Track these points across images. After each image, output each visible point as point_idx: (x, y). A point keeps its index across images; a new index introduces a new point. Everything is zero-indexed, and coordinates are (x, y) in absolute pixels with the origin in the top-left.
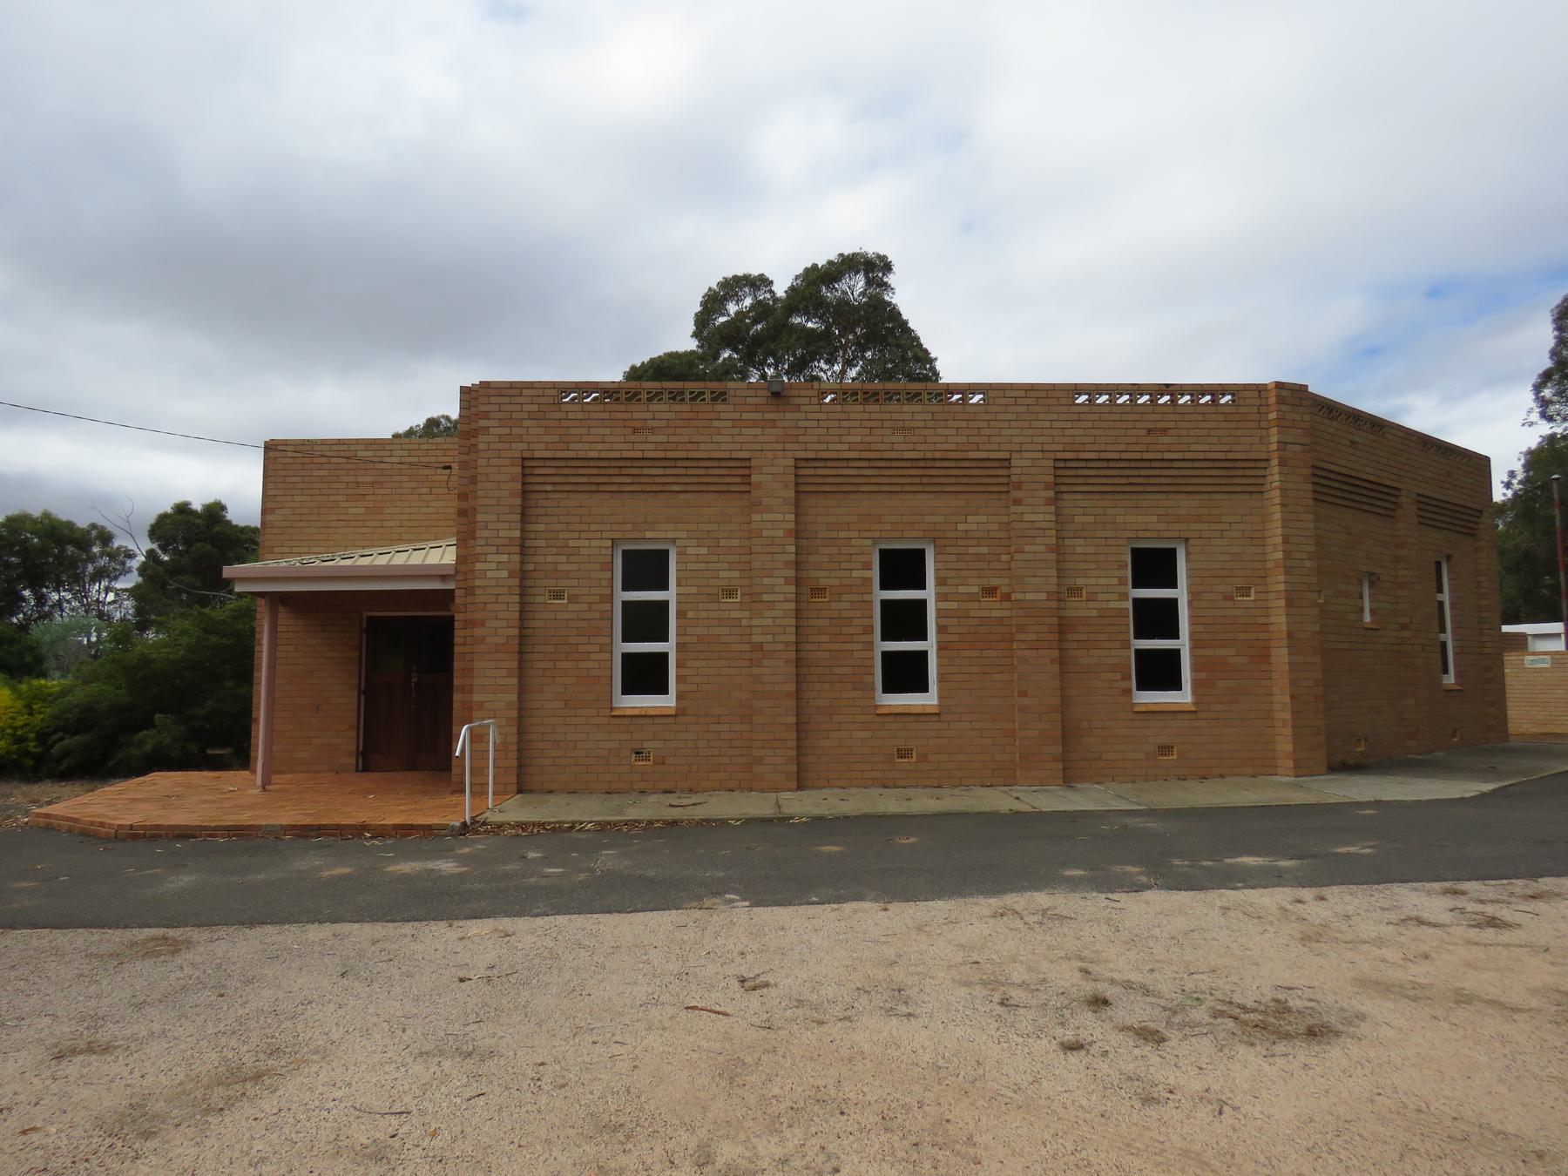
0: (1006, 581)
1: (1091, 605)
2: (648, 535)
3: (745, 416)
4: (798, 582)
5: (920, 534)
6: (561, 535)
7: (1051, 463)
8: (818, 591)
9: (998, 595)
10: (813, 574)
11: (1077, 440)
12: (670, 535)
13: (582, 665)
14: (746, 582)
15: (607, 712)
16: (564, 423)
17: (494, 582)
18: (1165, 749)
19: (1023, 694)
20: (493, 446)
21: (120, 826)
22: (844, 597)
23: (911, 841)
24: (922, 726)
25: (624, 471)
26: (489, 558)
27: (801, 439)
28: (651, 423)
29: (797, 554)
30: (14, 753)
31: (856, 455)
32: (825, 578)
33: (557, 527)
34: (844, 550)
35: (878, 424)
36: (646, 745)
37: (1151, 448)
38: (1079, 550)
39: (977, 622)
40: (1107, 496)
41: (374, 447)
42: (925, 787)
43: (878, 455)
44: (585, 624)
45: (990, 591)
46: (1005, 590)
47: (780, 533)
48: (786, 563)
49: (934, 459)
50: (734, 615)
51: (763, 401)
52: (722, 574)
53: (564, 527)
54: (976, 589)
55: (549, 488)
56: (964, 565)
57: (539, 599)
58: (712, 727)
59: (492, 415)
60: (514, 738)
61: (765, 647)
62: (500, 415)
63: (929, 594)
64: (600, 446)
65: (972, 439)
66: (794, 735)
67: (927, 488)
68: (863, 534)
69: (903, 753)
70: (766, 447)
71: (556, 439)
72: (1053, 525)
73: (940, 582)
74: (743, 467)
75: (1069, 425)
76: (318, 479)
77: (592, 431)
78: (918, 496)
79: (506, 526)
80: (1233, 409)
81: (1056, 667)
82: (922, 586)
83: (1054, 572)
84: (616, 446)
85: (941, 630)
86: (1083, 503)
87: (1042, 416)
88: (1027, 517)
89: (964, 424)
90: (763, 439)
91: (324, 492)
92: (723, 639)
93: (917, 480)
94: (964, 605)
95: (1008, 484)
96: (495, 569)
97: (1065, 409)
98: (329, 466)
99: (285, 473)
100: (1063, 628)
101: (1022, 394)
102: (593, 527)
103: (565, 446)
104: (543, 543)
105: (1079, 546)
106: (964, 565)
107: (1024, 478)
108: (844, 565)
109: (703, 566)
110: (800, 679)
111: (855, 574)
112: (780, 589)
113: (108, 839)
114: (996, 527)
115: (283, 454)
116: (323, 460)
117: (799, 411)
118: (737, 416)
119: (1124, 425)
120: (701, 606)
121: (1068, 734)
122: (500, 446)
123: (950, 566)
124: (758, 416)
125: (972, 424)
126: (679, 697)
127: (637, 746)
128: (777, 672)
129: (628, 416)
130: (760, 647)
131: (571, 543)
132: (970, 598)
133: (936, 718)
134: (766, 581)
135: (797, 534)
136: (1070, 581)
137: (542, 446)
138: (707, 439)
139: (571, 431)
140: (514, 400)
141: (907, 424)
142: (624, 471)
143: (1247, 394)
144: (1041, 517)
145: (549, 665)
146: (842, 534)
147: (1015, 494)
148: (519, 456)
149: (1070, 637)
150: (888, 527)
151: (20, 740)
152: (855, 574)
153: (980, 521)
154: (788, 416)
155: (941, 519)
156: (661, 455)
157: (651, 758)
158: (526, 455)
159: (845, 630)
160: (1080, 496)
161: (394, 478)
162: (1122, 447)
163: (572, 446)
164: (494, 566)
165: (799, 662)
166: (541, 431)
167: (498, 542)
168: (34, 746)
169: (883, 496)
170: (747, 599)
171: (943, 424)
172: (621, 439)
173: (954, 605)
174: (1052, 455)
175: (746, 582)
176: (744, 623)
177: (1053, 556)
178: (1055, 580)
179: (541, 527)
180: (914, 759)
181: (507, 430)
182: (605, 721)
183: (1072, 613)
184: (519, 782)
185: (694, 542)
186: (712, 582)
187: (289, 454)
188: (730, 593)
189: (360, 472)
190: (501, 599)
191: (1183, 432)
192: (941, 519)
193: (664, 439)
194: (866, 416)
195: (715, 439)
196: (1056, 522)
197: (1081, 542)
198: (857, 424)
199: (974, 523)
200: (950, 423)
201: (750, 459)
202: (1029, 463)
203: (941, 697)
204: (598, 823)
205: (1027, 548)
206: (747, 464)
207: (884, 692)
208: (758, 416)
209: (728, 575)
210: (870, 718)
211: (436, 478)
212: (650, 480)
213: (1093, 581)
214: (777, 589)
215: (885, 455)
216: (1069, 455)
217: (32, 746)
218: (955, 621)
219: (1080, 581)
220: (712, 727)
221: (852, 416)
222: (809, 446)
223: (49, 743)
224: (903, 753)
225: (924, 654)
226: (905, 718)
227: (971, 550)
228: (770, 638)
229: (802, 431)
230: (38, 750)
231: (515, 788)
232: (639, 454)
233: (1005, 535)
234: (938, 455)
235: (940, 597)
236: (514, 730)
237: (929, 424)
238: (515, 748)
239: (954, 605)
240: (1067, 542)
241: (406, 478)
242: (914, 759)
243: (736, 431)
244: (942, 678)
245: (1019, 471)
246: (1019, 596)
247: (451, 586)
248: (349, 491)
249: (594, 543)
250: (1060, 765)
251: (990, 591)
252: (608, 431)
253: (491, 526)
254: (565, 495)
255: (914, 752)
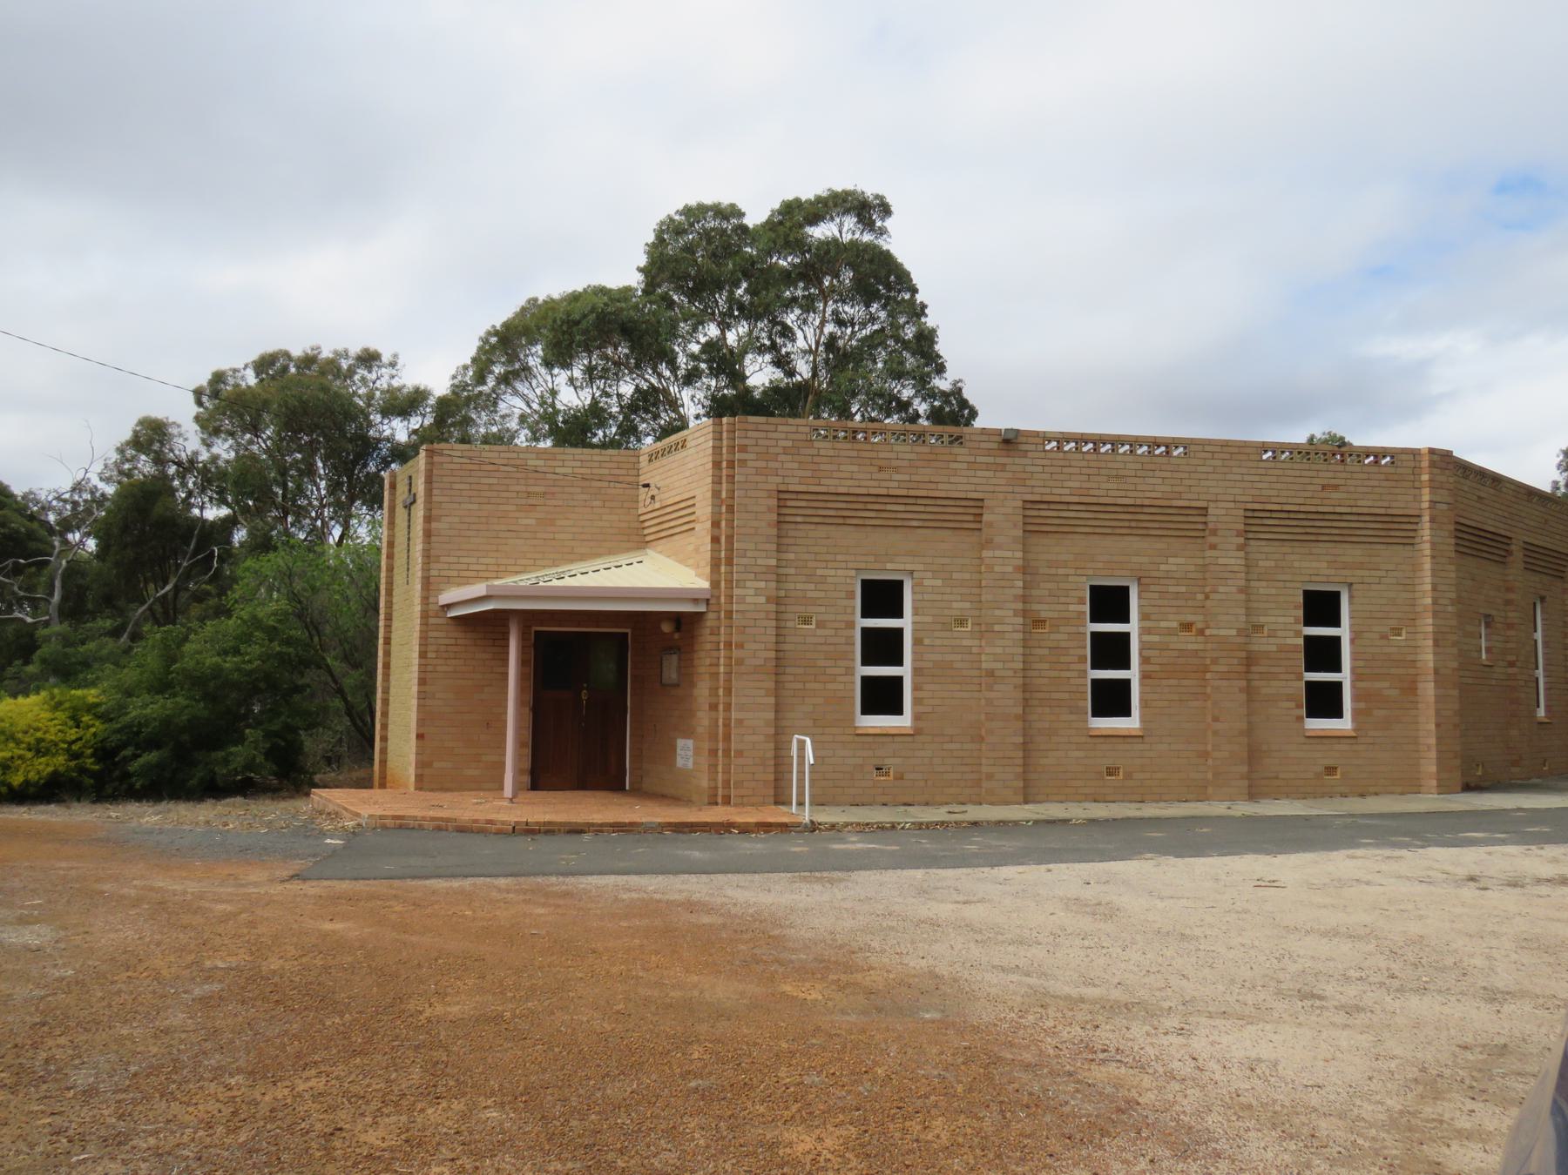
0: (1201, 618)
1: (1272, 640)
2: (889, 566)
3: (979, 459)
4: (1025, 613)
5: (1128, 573)
6: (810, 564)
7: (1242, 512)
8: (1039, 622)
9: (1194, 630)
10: (1035, 607)
11: (1264, 492)
12: (909, 567)
13: (830, 686)
14: (977, 613)
15: (850, 731)
16: (816, 459)
17: (752, 607)
18: (1331, 770)
19: (1216, 719)
20: (751, 478)
21: (517, 823)
22: (1062, 629)
23: (1205, 830)
24: (1128, 747)
25: (870, 506)
26: (748, 584)
27: (1028, 483)
28: (895, 463)
29: (1024, 588)
30: (73, 770)
31: (1076, 499)
32: (1045, 611)
33: (806, 556)
34: (1062, 585)
35: (1096, 471)
36: (887, 761)
37: (1325, 502)
38: (1262, 591)
39: (1175, 654)
40: (1286, 543)
41: (545, 456)
42: (1131, 802)
43: (1094, 500)
44: (832, 648)
45: (1187, 626)
46: (1200, 625)
47: (1010, 569)
48: (1015, 596)
49: (1143, 506)
50: (965, 642)
51: (995, 446)
52: (955, 605)
53: (812, 557)
54: (1175, 624)
55: (799, 519)
56: (1166, 602)
57: (789, 624)
58: (946, 746)
59: (749, 449)
60: (770, 754)
61: (997, 673)
62: (757, 449)
63: (1133, 627)
64: (850, 483)
65: (1176, 489)
66: (1021, 754)
67: (1135, 532)
68: (1079, 572)
69: (1111, 771)
70: (998, 489)
71: (809, 473)
72: (1243, 569)
73: (1144, 617)
74: (976, 507)
75: (1257, 478)
76: (486, 487)
77: (842, 468)
78: (1127, 538)
79: (764, 554)
80: (1392, 470)
81: (1243, 697)
82: (1126, 620)
83: (1243, 611)
84: (863, 483)
85: (1144, 660)
86: (1266, 549)
87: (1235, 470)
88: (1221, 561)
89: (1168, 474)
90: (994, 481)
91: (493, 501)
92: (956, 665)
93: (1127, 524)
94: (1168, 639)
95: (1204, 530)
96: (752, 595)
97: (1255, 464)
98: (497, 474)
99: (452, 479)
100: (1250, 660)
101: (1218, 449)
102: (839, 558)
103: (817, 481)
104: (792, 571)
105: (1262, 588)
106: (1166, 602)
107: (1220, 526)
108: (1062, 600)
109: (939, 597)
110: (1026, 703)
111: (1072, 608)
112: (1009, 621)
113: (499, 832)
114: (1192, 568)
115: (449, 459)
116: (491, 467)
117: (1026, 457)
118: (972, 459)
119: (1301, 480)
120: (937, 634)
121: (1254, 755)
122: (758, 479)
123: (1153, 602)
124: (990, 460)
125: (1176, 475)
126: (917, 717)
127: (878, 762)
128: (1007, 696)
129: (874, 455)
130: (991, 673)
131: (819, 572)
132: (1170, 632)
133: (1140, 740)
134: (997, 612)
135: (1025, 569)
136: (1255, 619)
137: (796, 480)
138: (946, 479)
139: (823, 467)
140: (770, 435)
141: (1121, 473)
142: (870, 506)
143: (1404, 457)
144: (1233, 561)
145: (800, 686)
146: (1061, 571)
147: (1213, 540)
148: (775, 488)
149: (1254, 669)
150: (1100, 565)
151: (75, 756)
152: (1072, 608)
153: (1178, 561)
154: (1017, 460)
155: (1146, 560)
156: (904, 492)
157: (891, 773)
158: (782, 488)
159: (1062, 659)
160: (1263, 543)
161: (566, 489)
162: (1301, 501)
163: (823, 481)
164: (752, 592)
165: (1025, 688)
166: (796, 465)
167: (757, 569)
168: (91, 764)
169: (1096, 537)
170: (977, 628)
171: (1151, 474)
172: (869, 476)
173: (1156, 638)
174: (1243, 506)
175: (977, 613)
176: (975, 650)
177: (1243, 597)
178: (1243, 618)
179: (792, 556)
180: (1121, 777)
181: (763, 464)
182: (850, 738)
183: (1255, 648)
184: (776, 795)
185: (929, 574)
186: (947, 612)
187: (456, 460)
188: (961, 622)
189: (532, 482)
190: (758, 623)
191: (1352, 489)
192: (1146, 560)
193: (907, 477)
194: (1084, 464)
195: (952, 479)
196: (1246, 566)
197: (1264, 584)
198: (1077, 471)
199: (1175, 564)
200: (1157, 473)
201: (982, 500)
202: (1223, 512)
203: (1142, 721)
204: (913, 823)
205: (1221, 589)
206: (979, 504)
207: (1093, 716)
208: (990, 460)
209: (960, 607)
210: (1083, 739)
211: (609, 491)
212: (893, 515)
213: (1272, 619)
214: (1007, 620)
215: (1102, 500)
216: (1257, 506)
217: (90, 763)
218: (1156, 653)
219: (1262, 620)
220: (946, 746)
221: (1073, 463)
222: (1036, 490)
223: (117, 759)
224: (1111, 771)
225: (1127, 683)
226: (1114, 740)
227: (1171, 589)
228: (1000, 665)
229: (1029, 476)
230: (97, 767)
231: (772, 800)
232: (884, 492)
233: (1200, 575)
234: (1147, 502)
235: (1144, 631)
236: (772, 746)
237: (1139, 473)
238: (772, 763)
239: (1156, 638)
240: (1253, 584)
241: (579, 490)
242: (1121, 777)
243: (971, 473)
244: (1144, 704)
245: (1214, 519)
246: (1215, 632)
247: (702, 608)
248: (519, 501)
249: (840, 572)
250: (1246, 783)
251: (1187, 626)
252: (855, 468)
253: (749, 554)
254: (813, 527)
255: (1121, 770)
